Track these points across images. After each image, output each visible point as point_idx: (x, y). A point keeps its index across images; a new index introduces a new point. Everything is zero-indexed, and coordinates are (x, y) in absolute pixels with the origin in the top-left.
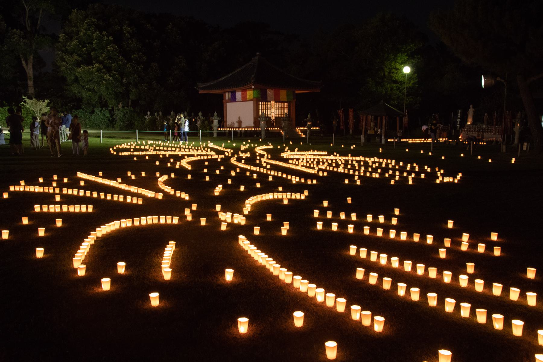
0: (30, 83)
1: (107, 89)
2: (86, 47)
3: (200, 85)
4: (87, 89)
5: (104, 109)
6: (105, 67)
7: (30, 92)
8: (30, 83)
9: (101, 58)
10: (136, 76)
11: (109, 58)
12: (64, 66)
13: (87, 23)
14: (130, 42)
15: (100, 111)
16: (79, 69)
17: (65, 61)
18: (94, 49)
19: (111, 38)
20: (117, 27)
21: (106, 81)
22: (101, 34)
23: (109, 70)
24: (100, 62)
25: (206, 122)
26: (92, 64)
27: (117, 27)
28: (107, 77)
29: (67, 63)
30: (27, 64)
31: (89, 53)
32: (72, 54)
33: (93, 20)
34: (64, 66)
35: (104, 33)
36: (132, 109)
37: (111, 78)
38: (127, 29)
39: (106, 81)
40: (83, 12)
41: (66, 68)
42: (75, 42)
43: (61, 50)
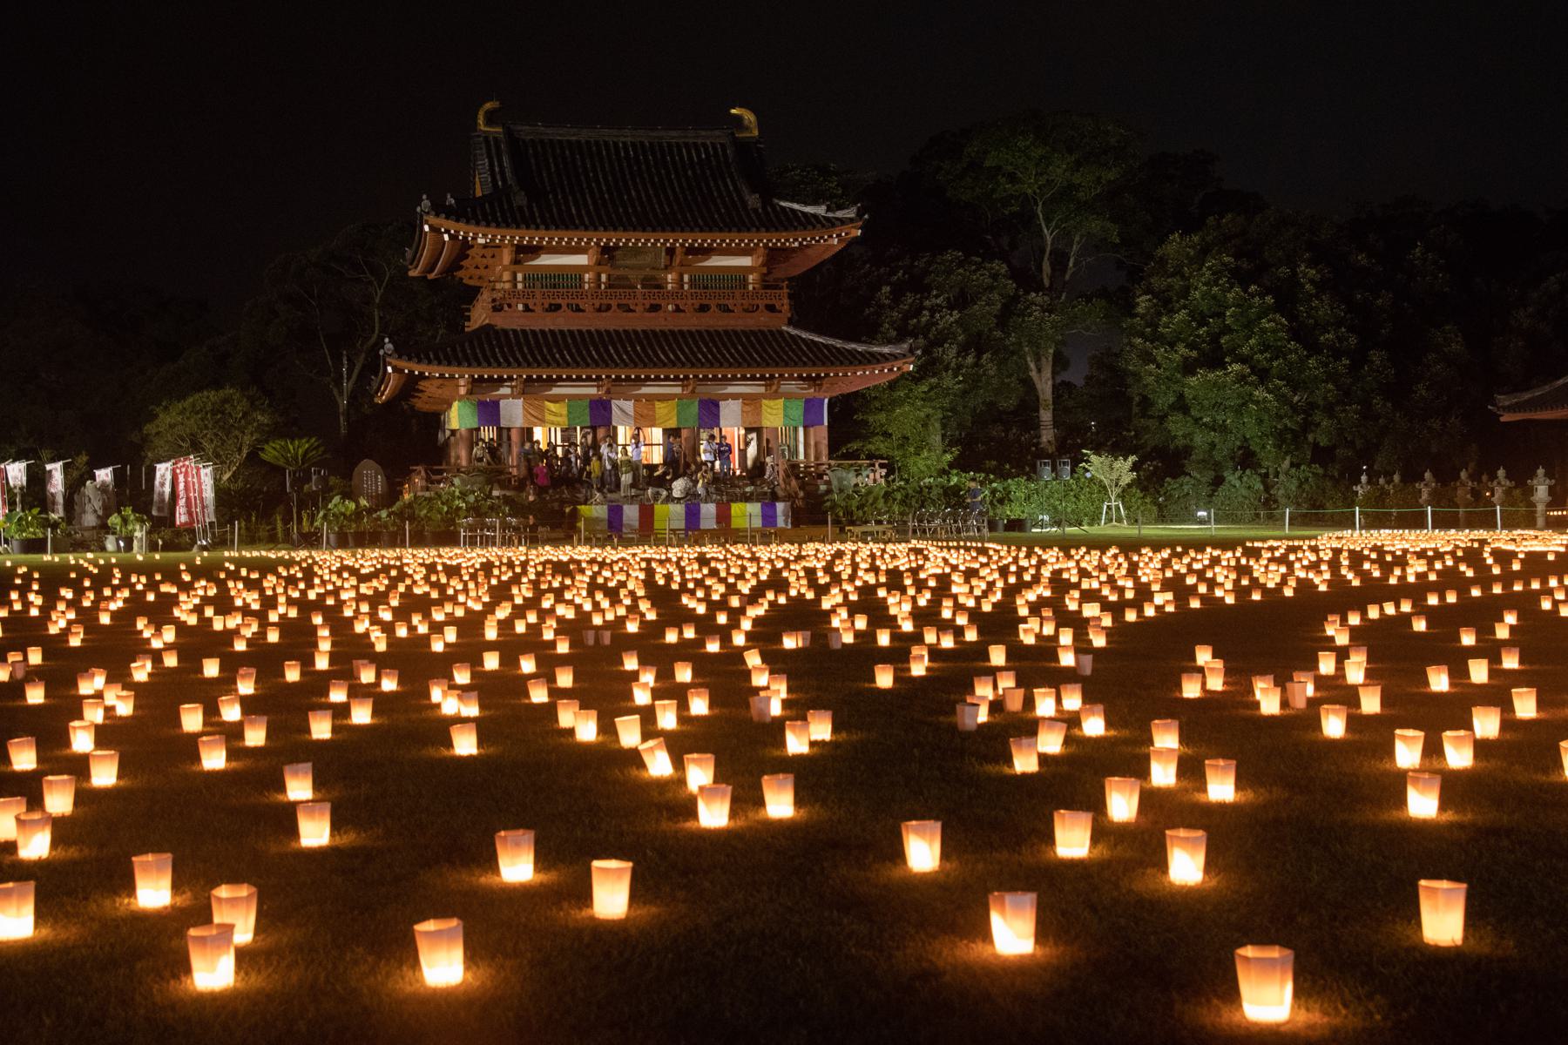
0: (1046, 416)
1: (1260, 422)
2: (1207, 324)
3: (1504, 400)
4: (1205, 424)
5: (1248, 472)
6: (1253, 372)
7: (1044, 439)
8: (1046, 416)
9: (1245, 350)
10: (1330, 386)
11: (1266, 347)
12: (1151, 374)
13: (1209, 268)
14: (1315, 303)
15: (1240, 478)
16: (1193, 381)
17: (1154, 361)
18: (1227, 330)
19: (1269, 299)
20: (1284, 271)
21: (1257, 403)
22: (1245, 291)
23: (1263, 376)
24: (1243, 360)
25: (1517, 492)
26: (1223, 366)
27: (1284, 271)
28: (1259, 393)
29: (1159, 367)
30: (1039, 371)
31: (1214, 339)
32: (1172, 345)
33: (1226, 259)
34: (1151, 374)
35: (1253, 288)
36: (1321, 471)
37: (1270, 397)
38: (1308, 273)
39: (1257, 403)
40: (1196, 239)
41: (1158, 377)
42: (1182, 315)
43: (1142, 335)
